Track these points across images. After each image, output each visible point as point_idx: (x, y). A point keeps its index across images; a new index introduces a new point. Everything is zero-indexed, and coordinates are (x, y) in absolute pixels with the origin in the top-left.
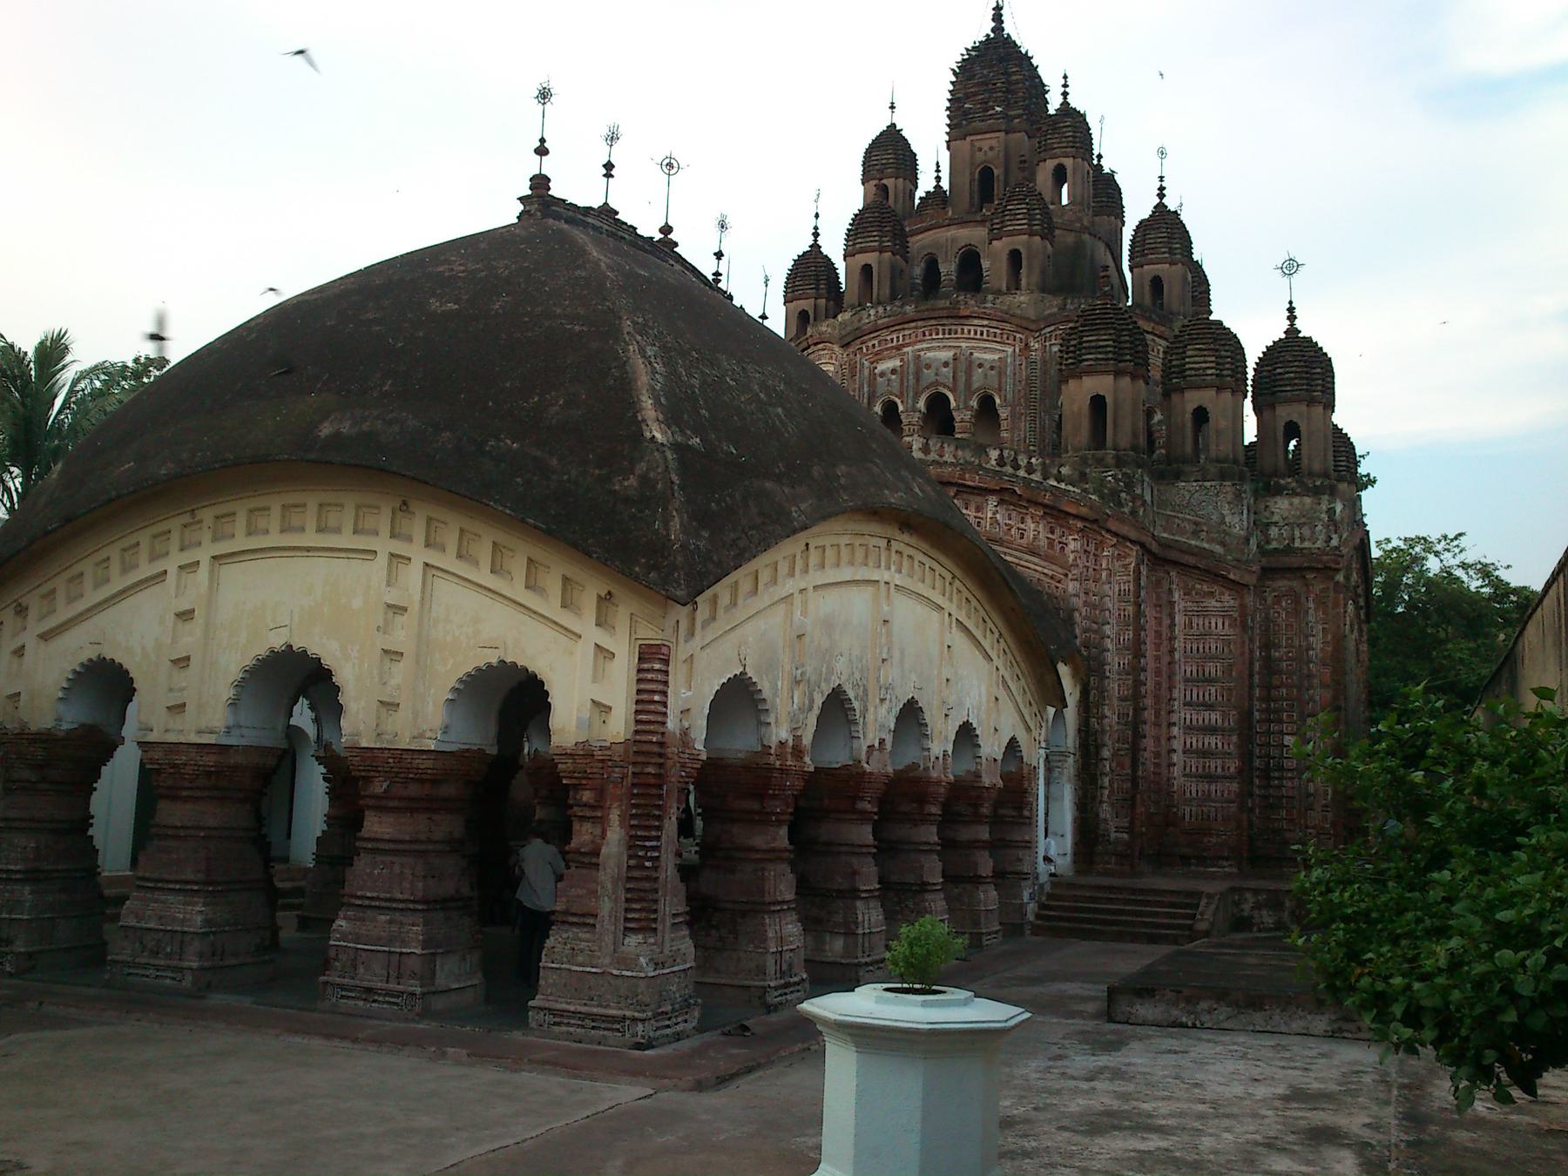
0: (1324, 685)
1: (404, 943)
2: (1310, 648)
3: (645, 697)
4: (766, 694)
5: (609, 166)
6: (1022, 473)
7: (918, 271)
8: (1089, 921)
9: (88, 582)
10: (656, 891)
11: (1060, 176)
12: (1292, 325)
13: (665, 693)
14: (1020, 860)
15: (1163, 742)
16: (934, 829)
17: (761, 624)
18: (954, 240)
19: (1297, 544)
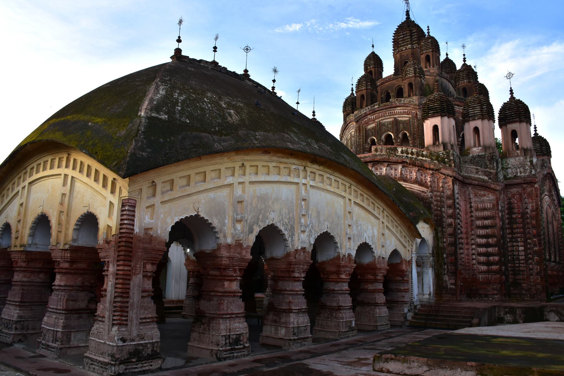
1: (58, 327)
5: (215, 48)
10: (127, 307)
12: (512, 96)
13: (134, 221)
14: (403, 297)
17: (211, 195)
19: (519, 174)
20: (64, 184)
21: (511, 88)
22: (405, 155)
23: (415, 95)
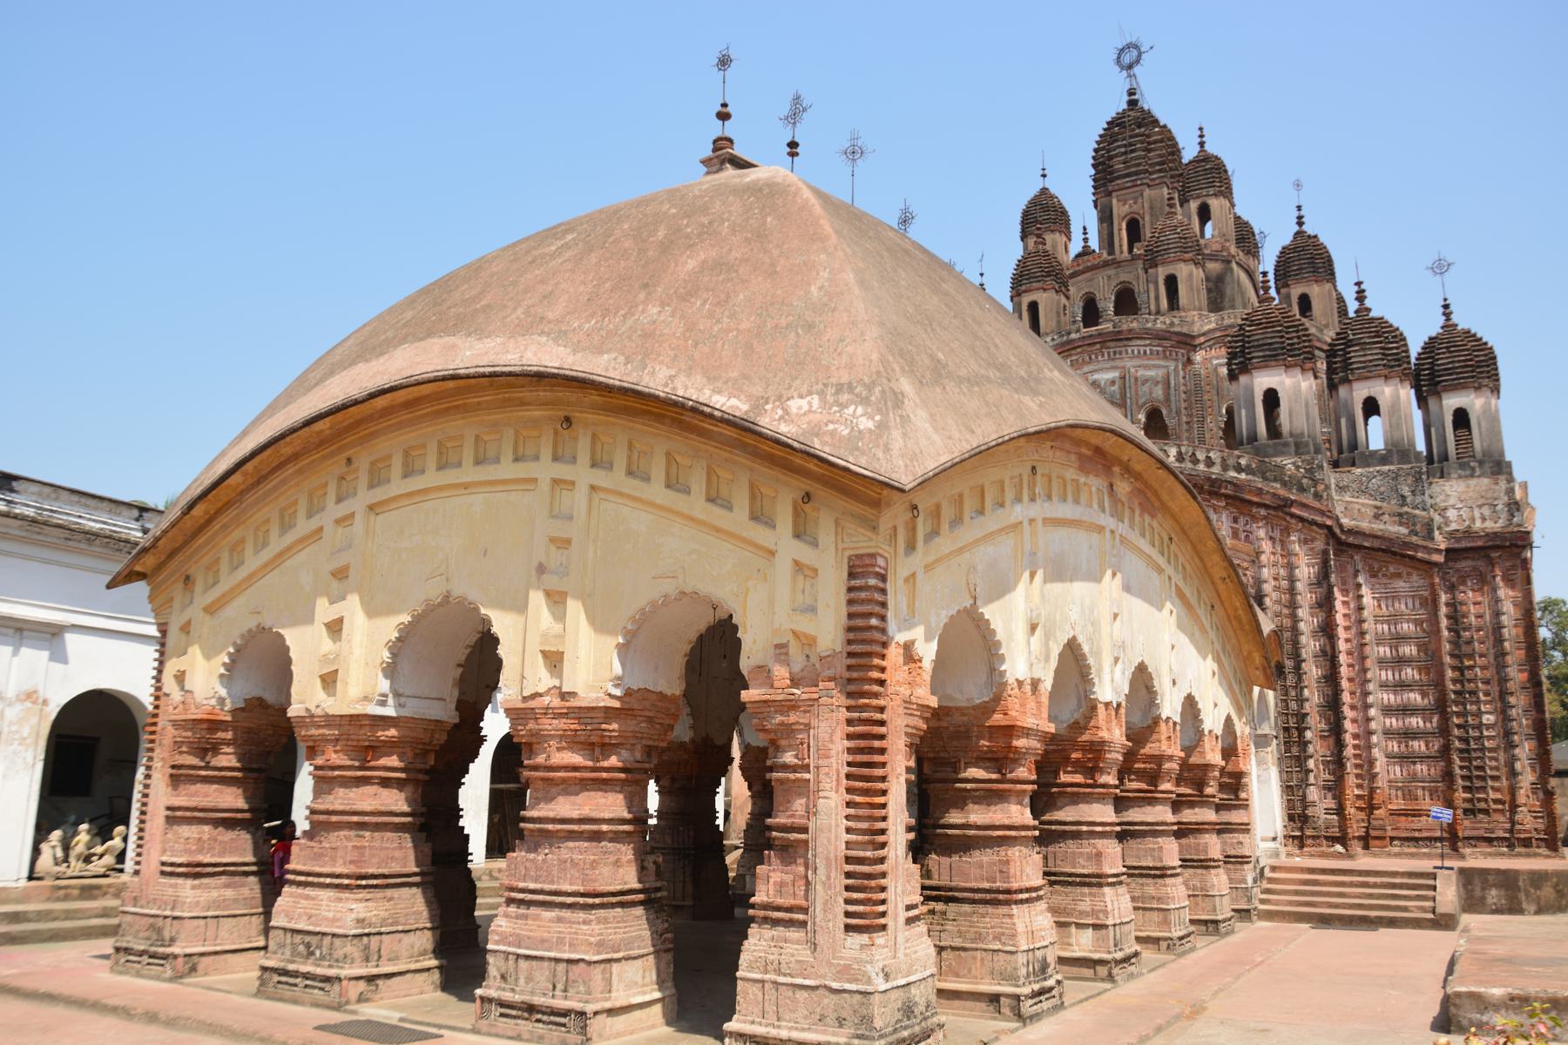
3: (860, 622)
4: (1000, 636)
5: (793, 145)
6: (1201, 467)
8: (1337, 906)
12: (1448, 319)
13: (883, 618)
22: (1190, 465)
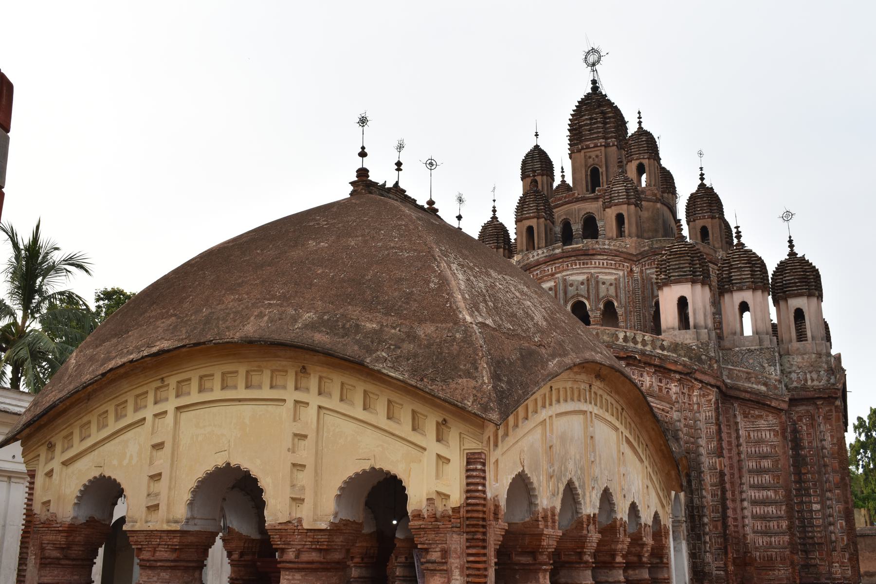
0: (834, 471)
2: (823, 448)
3: (472, 487)
4: (536, 485)
5: (399, 164)
7: (558, 229)
9: (94, 427)
11: (641, 170)
12: (792, 250)
13: (484, 485)
15: (739, 511)
16: (621, 572)
17: (530, 438)
18: (579, 210)
19: (809, 383)
20: (295, 420)
21: (790, 237)
22: (632, 345)
23: (630, 236)
